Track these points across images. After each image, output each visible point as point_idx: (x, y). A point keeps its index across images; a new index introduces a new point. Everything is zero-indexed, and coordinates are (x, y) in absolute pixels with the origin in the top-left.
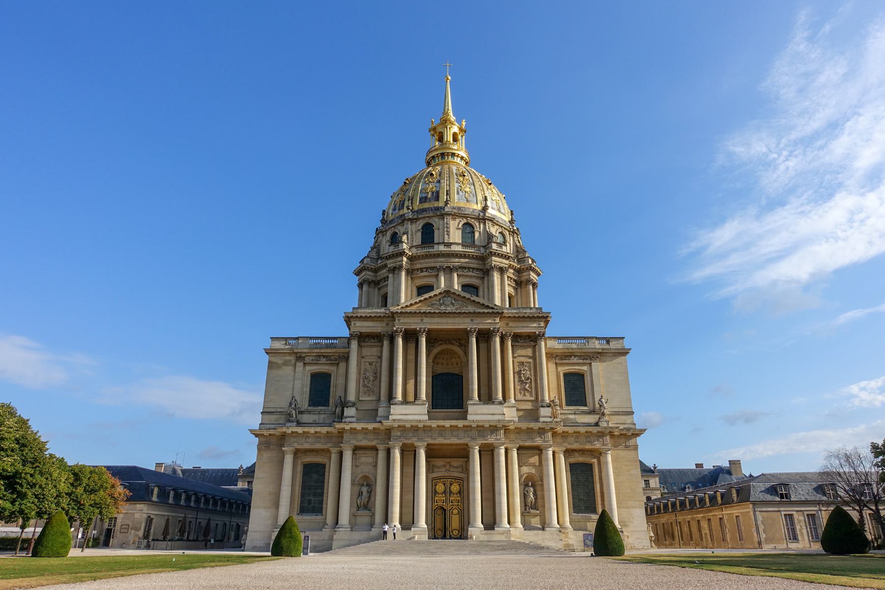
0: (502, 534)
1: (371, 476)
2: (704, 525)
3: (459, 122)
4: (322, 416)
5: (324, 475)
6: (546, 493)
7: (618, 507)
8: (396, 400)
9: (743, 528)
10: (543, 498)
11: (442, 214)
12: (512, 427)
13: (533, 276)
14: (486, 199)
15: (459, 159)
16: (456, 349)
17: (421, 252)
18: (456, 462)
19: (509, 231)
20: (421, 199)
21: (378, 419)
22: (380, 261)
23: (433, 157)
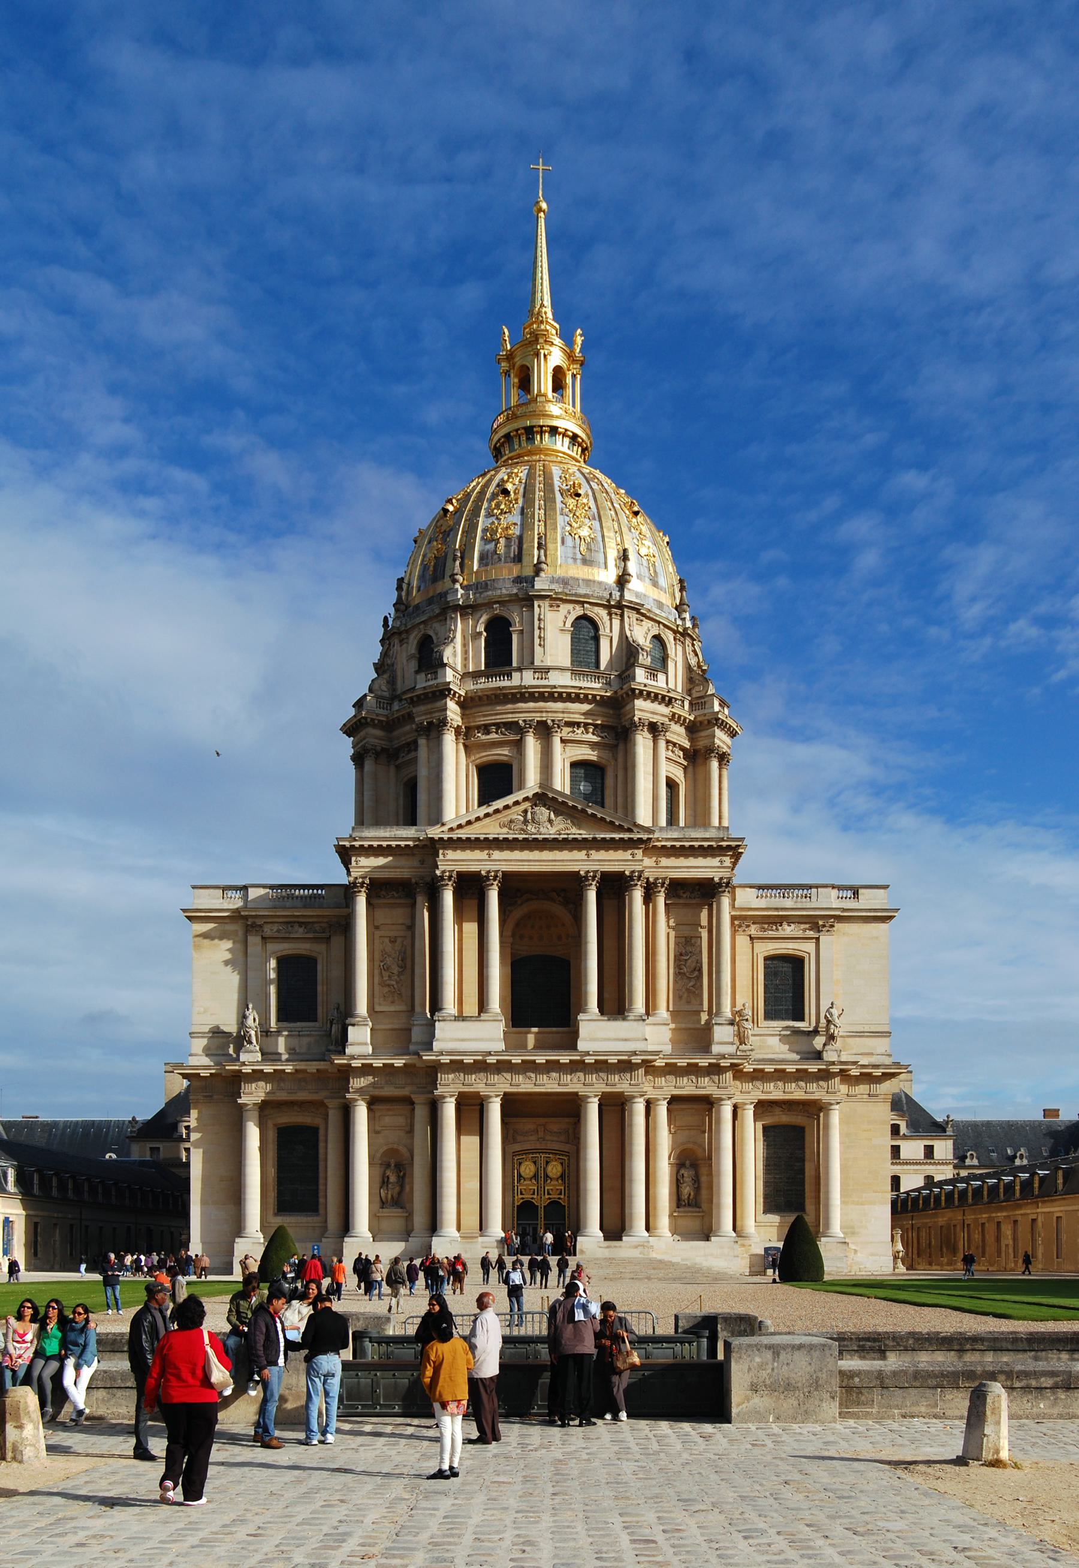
0: (636, 1247)
1: (403, 1150)
2: (1007, 1230)
3: (567, 337)
4: (305, 1040)
5: (316, 1147)
6: (715, 1180)
7: (842, 1202)
8: (444, 1013)
9: (1064, 1237)
10: (710, 1187)
11: (527, 600)
12: (660, 1063)
13: (721, 738)
14: (624, 557)
15: (567, 440)
16: (558, 910)
17: (484, 684)
18: (557, 1125)
19: (675, 632)
20: (483, 558)
21: (412, 1048)
22: (396, 706)
23: (507, 436)
